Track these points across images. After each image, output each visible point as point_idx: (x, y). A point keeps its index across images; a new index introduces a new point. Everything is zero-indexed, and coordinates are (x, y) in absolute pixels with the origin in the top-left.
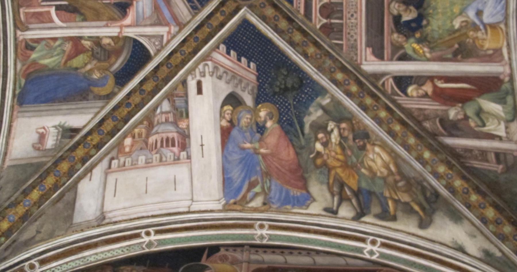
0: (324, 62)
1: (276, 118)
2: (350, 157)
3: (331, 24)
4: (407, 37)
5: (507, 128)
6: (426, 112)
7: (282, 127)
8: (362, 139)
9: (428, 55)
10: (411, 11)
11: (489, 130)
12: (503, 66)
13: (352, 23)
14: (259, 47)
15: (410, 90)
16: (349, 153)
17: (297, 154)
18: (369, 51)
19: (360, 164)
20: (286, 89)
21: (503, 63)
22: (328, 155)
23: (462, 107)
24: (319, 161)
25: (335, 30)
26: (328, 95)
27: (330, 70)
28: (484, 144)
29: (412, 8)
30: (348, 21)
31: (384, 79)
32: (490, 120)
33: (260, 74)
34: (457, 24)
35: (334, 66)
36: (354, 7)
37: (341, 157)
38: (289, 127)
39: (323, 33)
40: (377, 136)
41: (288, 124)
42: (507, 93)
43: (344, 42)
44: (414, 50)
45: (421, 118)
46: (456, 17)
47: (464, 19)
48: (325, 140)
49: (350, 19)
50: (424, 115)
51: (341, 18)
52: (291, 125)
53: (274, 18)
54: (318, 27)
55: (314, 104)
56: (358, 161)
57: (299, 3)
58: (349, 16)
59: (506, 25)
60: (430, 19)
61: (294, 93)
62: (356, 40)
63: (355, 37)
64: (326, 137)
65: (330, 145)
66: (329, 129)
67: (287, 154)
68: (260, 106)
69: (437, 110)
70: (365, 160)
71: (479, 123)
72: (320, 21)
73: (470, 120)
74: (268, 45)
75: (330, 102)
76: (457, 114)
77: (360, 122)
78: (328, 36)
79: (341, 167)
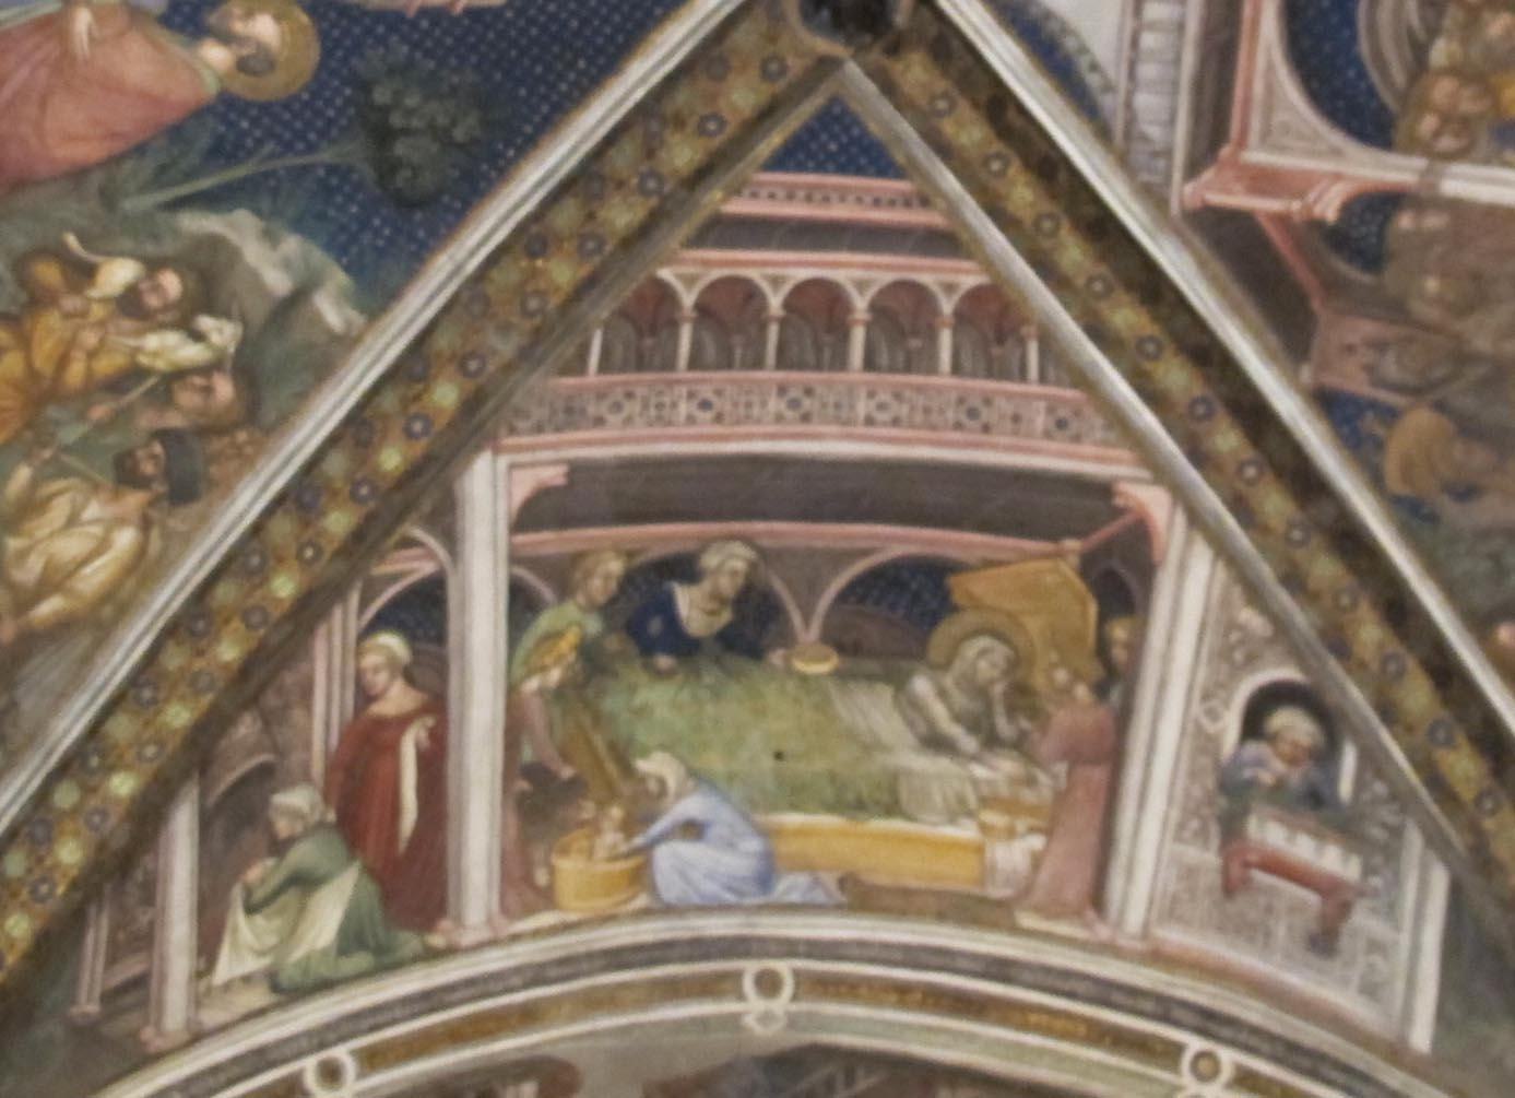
0: (505, 329)
1: (241, 86)
2: (81, 416)
3: (674, 325)
4: (607, 610)
5: (247, 980)
6: (297, 714)
7: (201, 113)
8: (167, 474)
9: (532, 684)
10: (712, 613)
11: (235, 930)
12: (489, 921)
13: (674, 405)
14: (584, 22)
15: (392, 643)
16: (99, 412)
17: (78, 175)
18: (554, 475)
19: (55, 459)
20: (383, 136)
21: (500, 921)
22: (84, 314)
23: (321, 825)
24: (48, 273)
25: (649, 342)
26: (358, 319)
27: (472, 355)
28: (179, 929)
29: (726, 617)
30: (684, 390)
31: (432, 542)
32: (277, 923)
33: (456, 21)
34: (656, 765)
35: (491, 367)
36: (742, 411)
37: (76, 372)
38: (204, 142)
39: (639, 297)
40: (187, 540)
41: (220, 139)
42: (380, 950)
43: (592, 376)
44: (554, 636)
45: (271, 700)
46: (682, 760)
47: (672, 783)
48: (153, 301)
49: (691, 395)
50: (286, 707)
51: (695, 363)
52: (221, 153)
53: (716, 117)
54: (666, 274)
55: (318, 256)
56: (67, 449)
57: (772, 196)
58: (706, 392)
59: (646, 913)
60: (679, 678)
61: (367, 172)
62: (599, 422)
63: (612, 419)
64: (166, 308)
65: (127, 324)
66: (206, 323)
67: (71, 132)
68: (304, 19)
69: (308, 745)
70: (72, 481)
71: (259, 894)
72: (690, 281)
73: (270, 862)
74: (591, 61)
75: (329, 332)
76: (295, 814)
77: (246, 461)
78: (623, 313)
79: (32, 373)
